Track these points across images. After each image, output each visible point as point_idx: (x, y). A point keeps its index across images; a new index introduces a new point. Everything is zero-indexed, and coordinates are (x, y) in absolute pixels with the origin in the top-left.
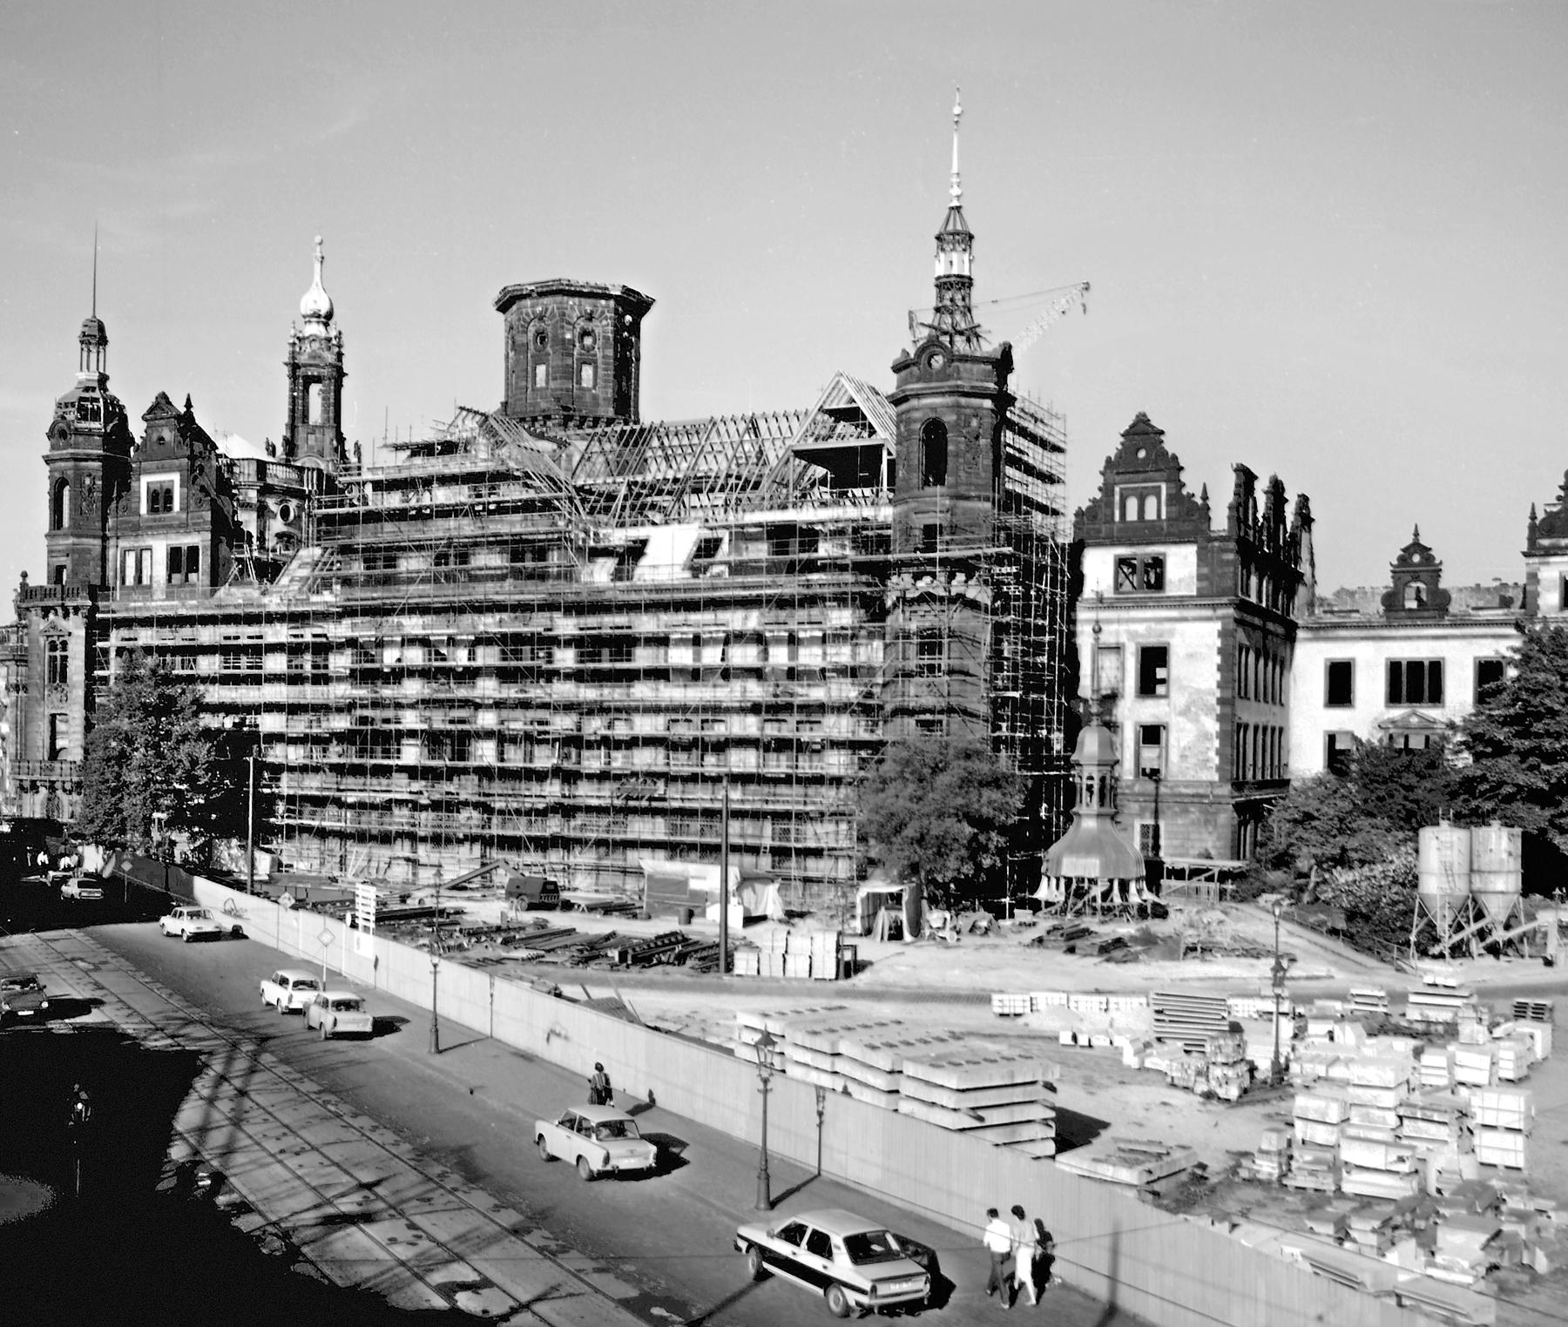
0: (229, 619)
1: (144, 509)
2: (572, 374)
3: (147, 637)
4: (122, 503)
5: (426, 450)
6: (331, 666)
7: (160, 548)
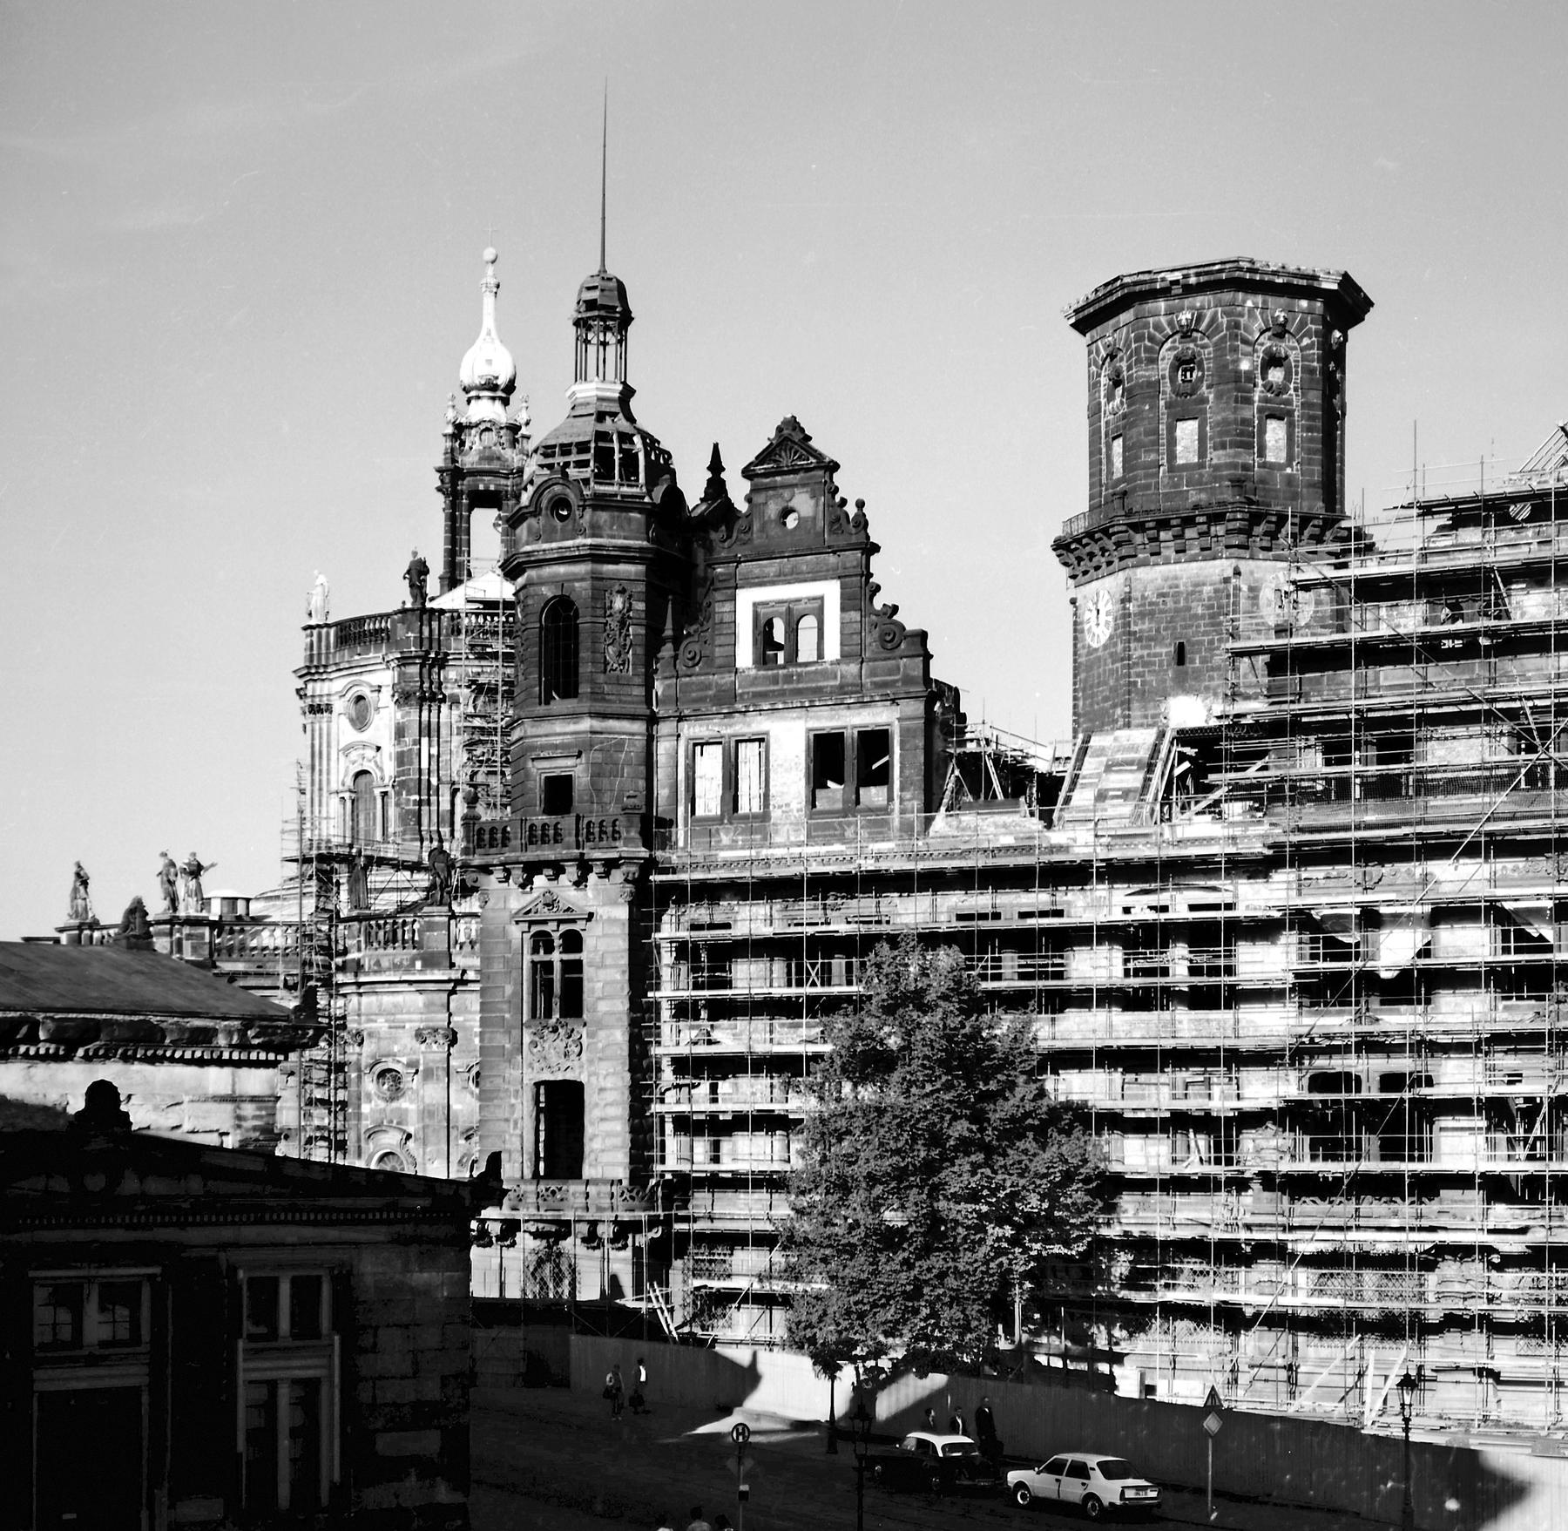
0: (965, 880)
1: (745, 655)
2: (1247, 437)
3: (753, 920)
4: (691, 647)
5: (1488, 511)
6: (1241, 969)
7: (789, 736)
